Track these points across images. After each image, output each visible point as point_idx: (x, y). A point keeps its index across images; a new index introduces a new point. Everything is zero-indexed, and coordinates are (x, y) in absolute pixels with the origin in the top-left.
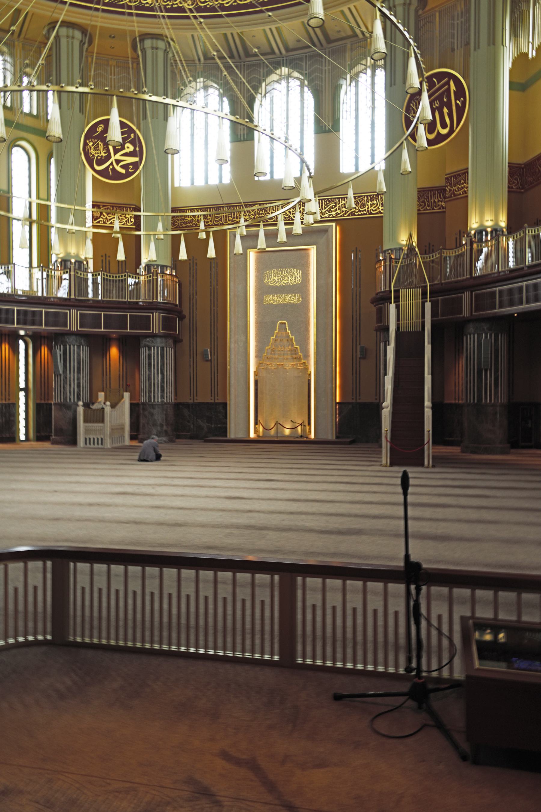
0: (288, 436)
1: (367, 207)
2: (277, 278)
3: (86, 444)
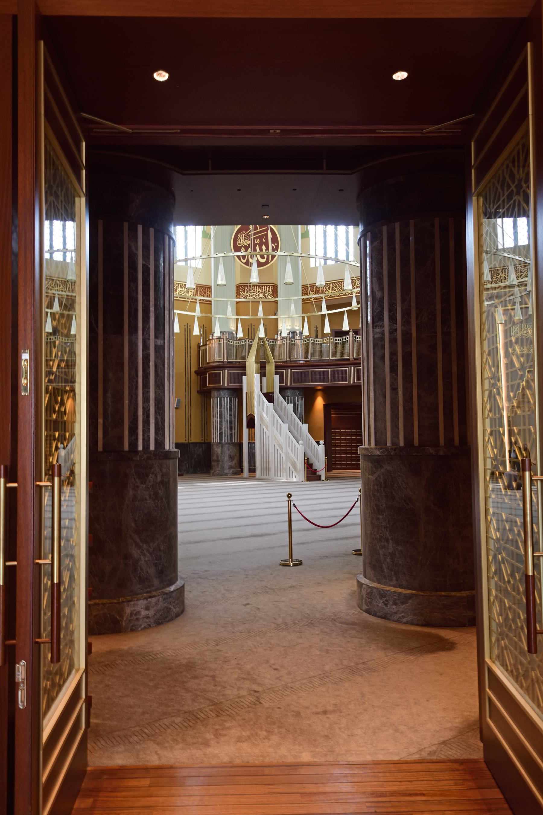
1: (178, 292)
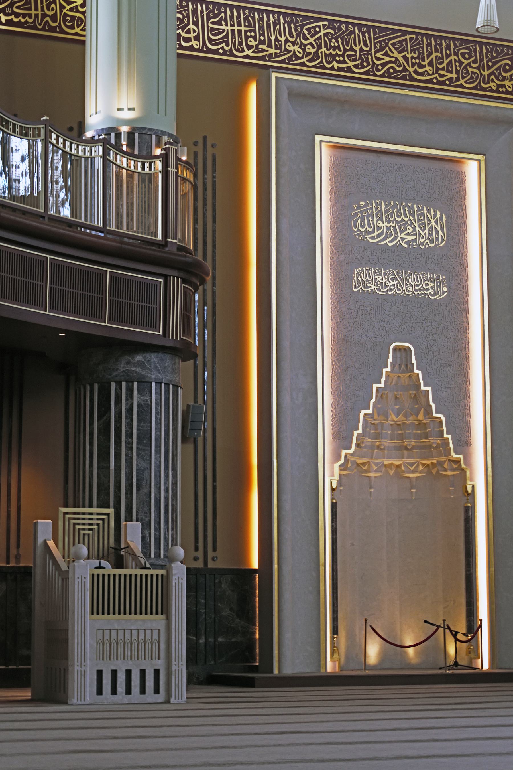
0: (374, 668)
2: (386, 223)
3: (100, 692)
